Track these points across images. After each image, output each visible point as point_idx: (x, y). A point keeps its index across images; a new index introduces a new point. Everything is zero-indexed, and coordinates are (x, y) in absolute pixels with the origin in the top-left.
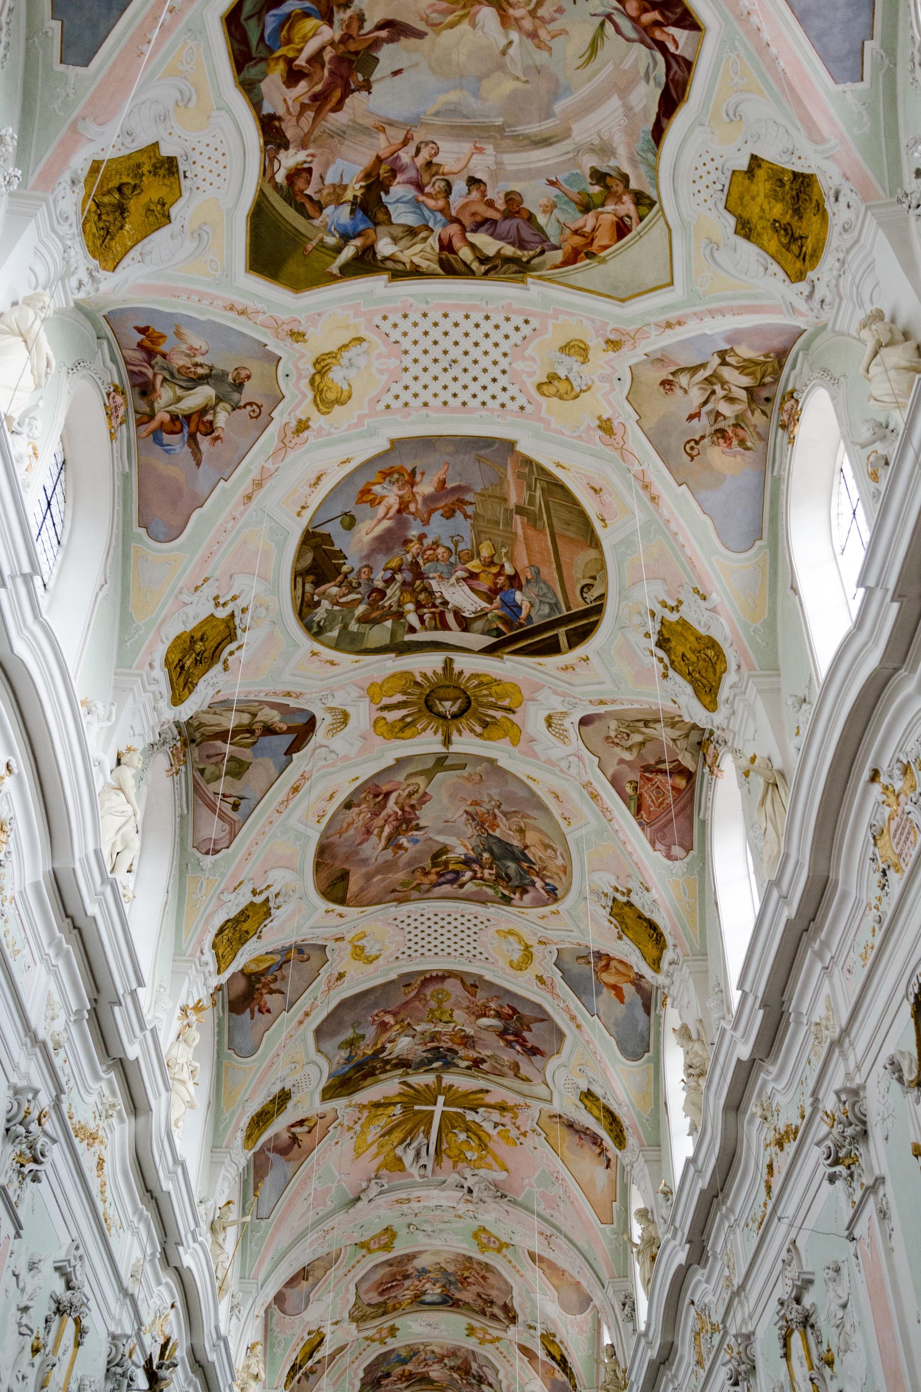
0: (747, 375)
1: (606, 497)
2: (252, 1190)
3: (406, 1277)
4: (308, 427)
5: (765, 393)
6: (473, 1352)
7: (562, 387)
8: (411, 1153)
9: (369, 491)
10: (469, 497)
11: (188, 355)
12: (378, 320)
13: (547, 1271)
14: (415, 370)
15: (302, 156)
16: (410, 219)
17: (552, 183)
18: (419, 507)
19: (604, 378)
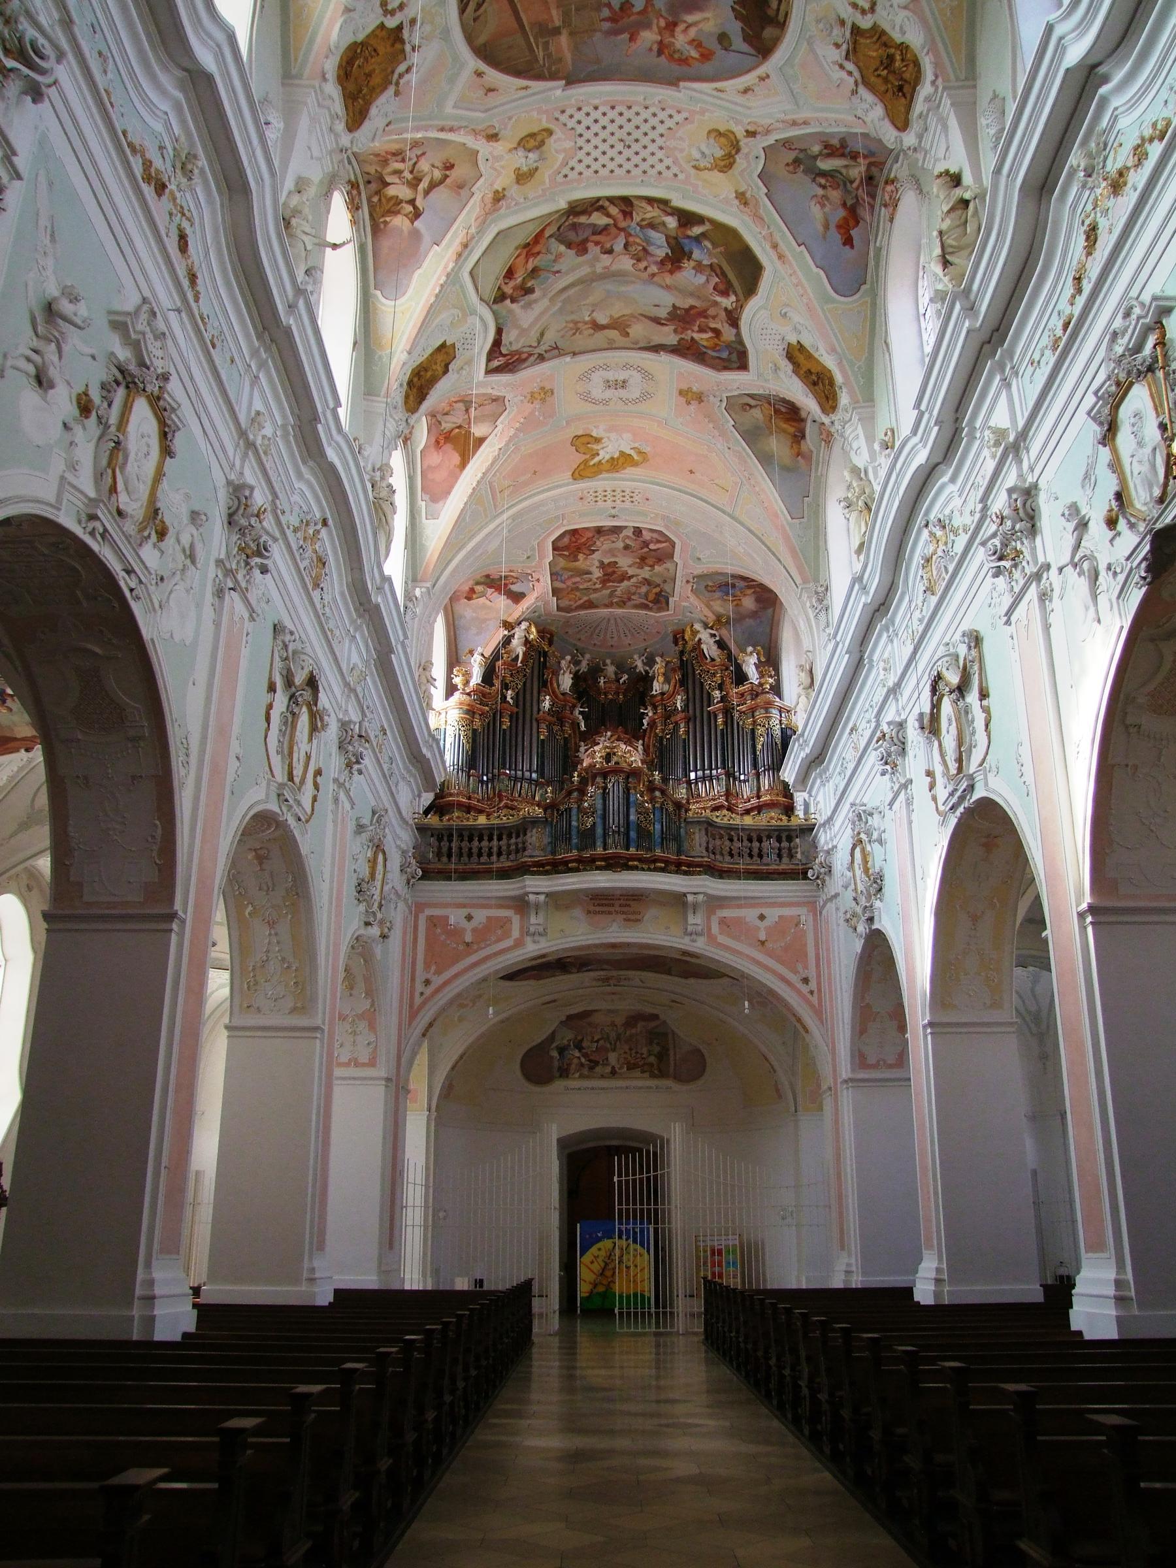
0: (392, 198)
1: (481, 92)
4: (747, 131)
5: (374, 186)
7: (532, 143)
9: (702, 55)
10: (607, 25)
11: (828, 199)
12: (681, 176)
14: (653, 135)
15: (719, 299)
16: (653, 234)
17: (558, 272)
18: (655, 21)
19: (498, 158)
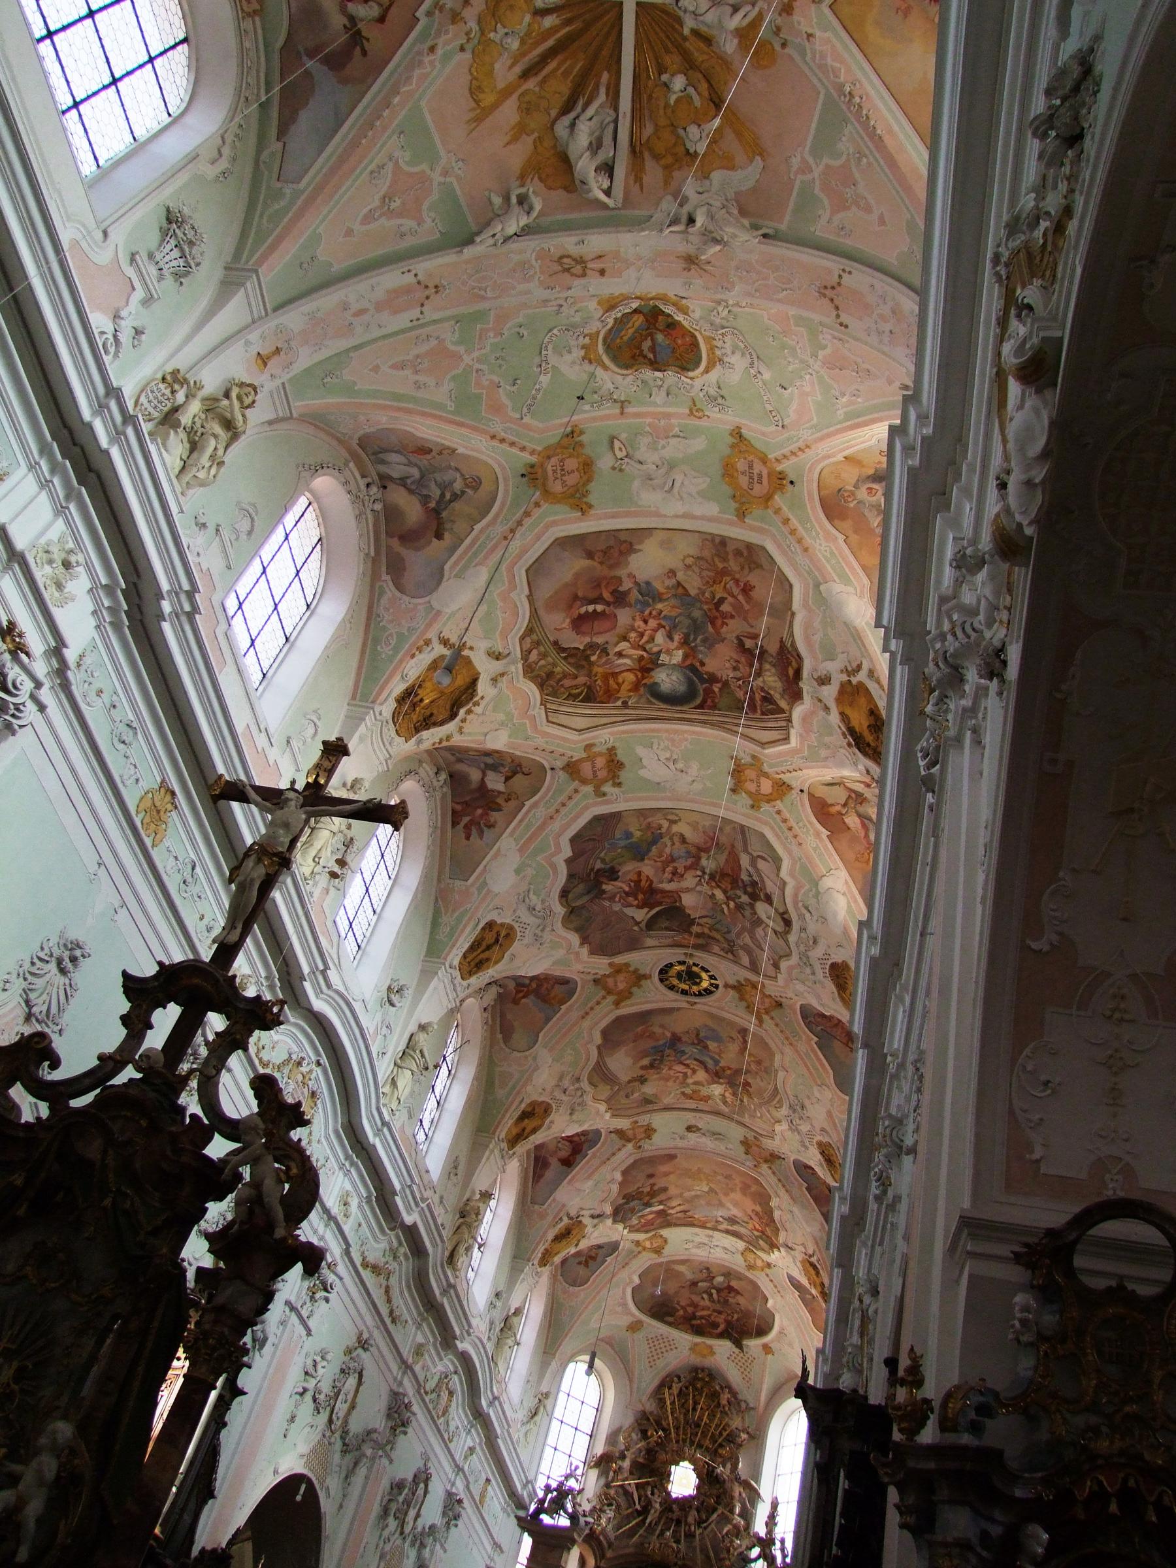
2: (273, 132)
3: (620, 599)
6: (742, 827)
8: (583, 137)
13: (854, 538)
